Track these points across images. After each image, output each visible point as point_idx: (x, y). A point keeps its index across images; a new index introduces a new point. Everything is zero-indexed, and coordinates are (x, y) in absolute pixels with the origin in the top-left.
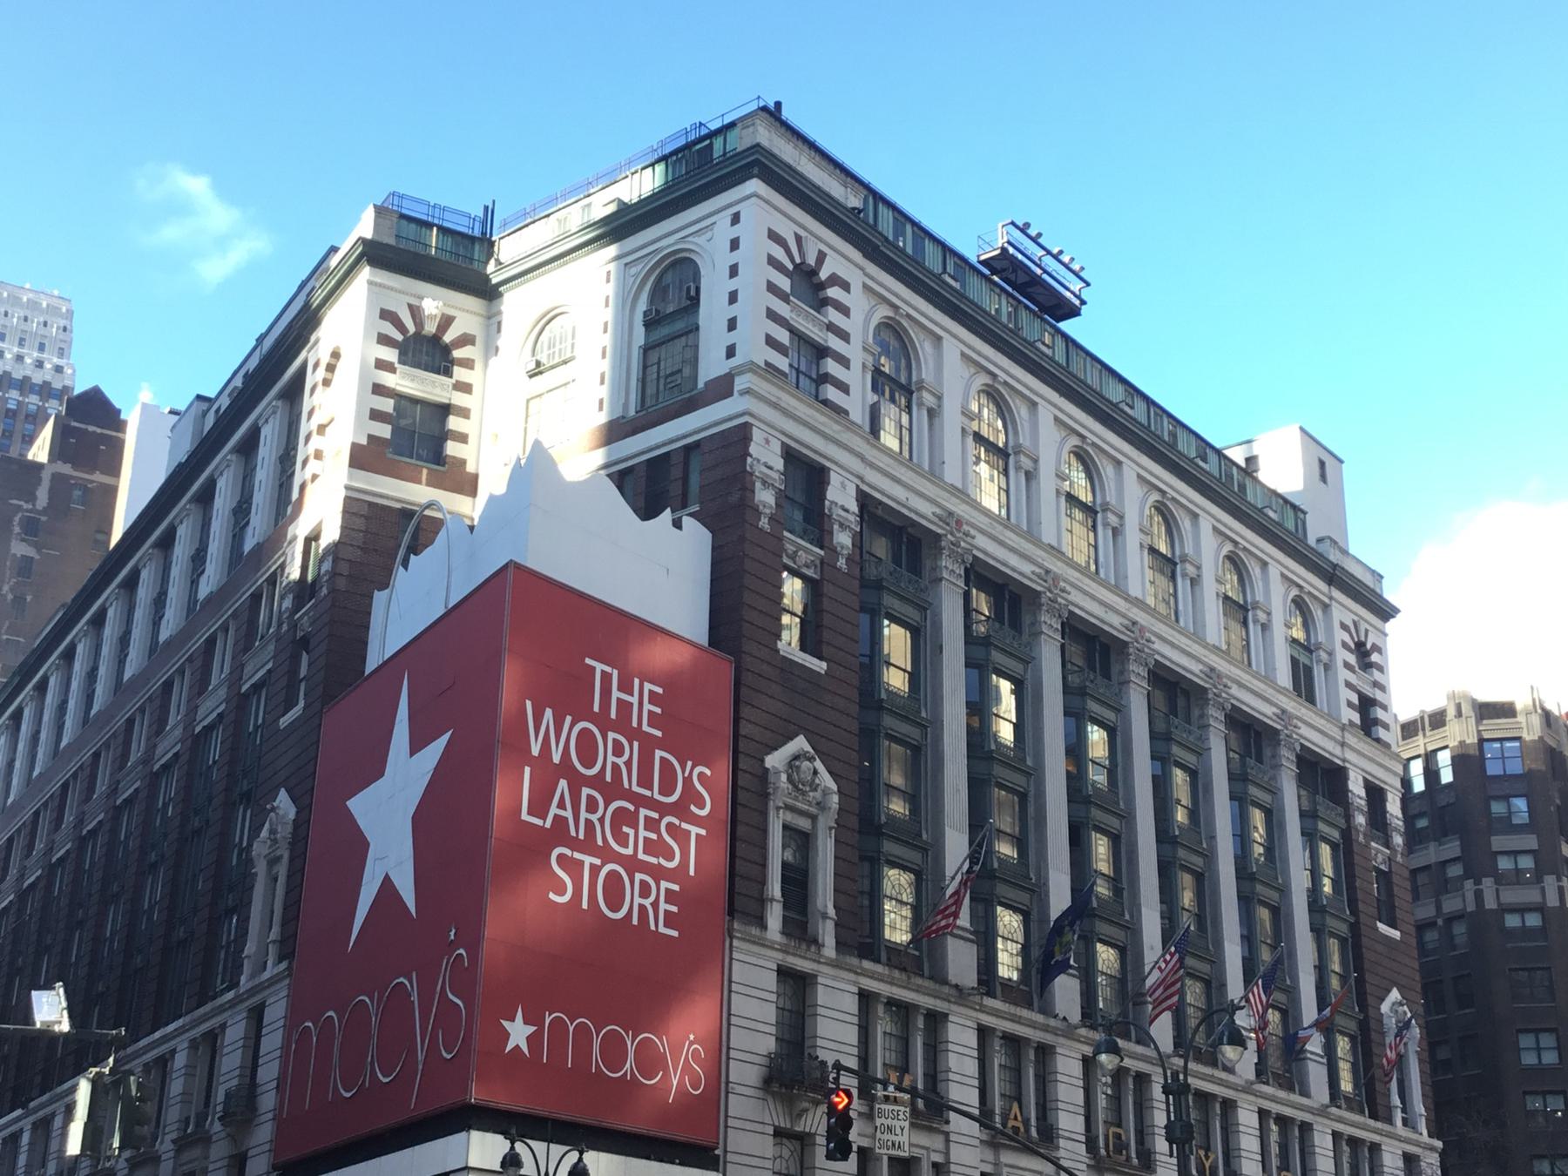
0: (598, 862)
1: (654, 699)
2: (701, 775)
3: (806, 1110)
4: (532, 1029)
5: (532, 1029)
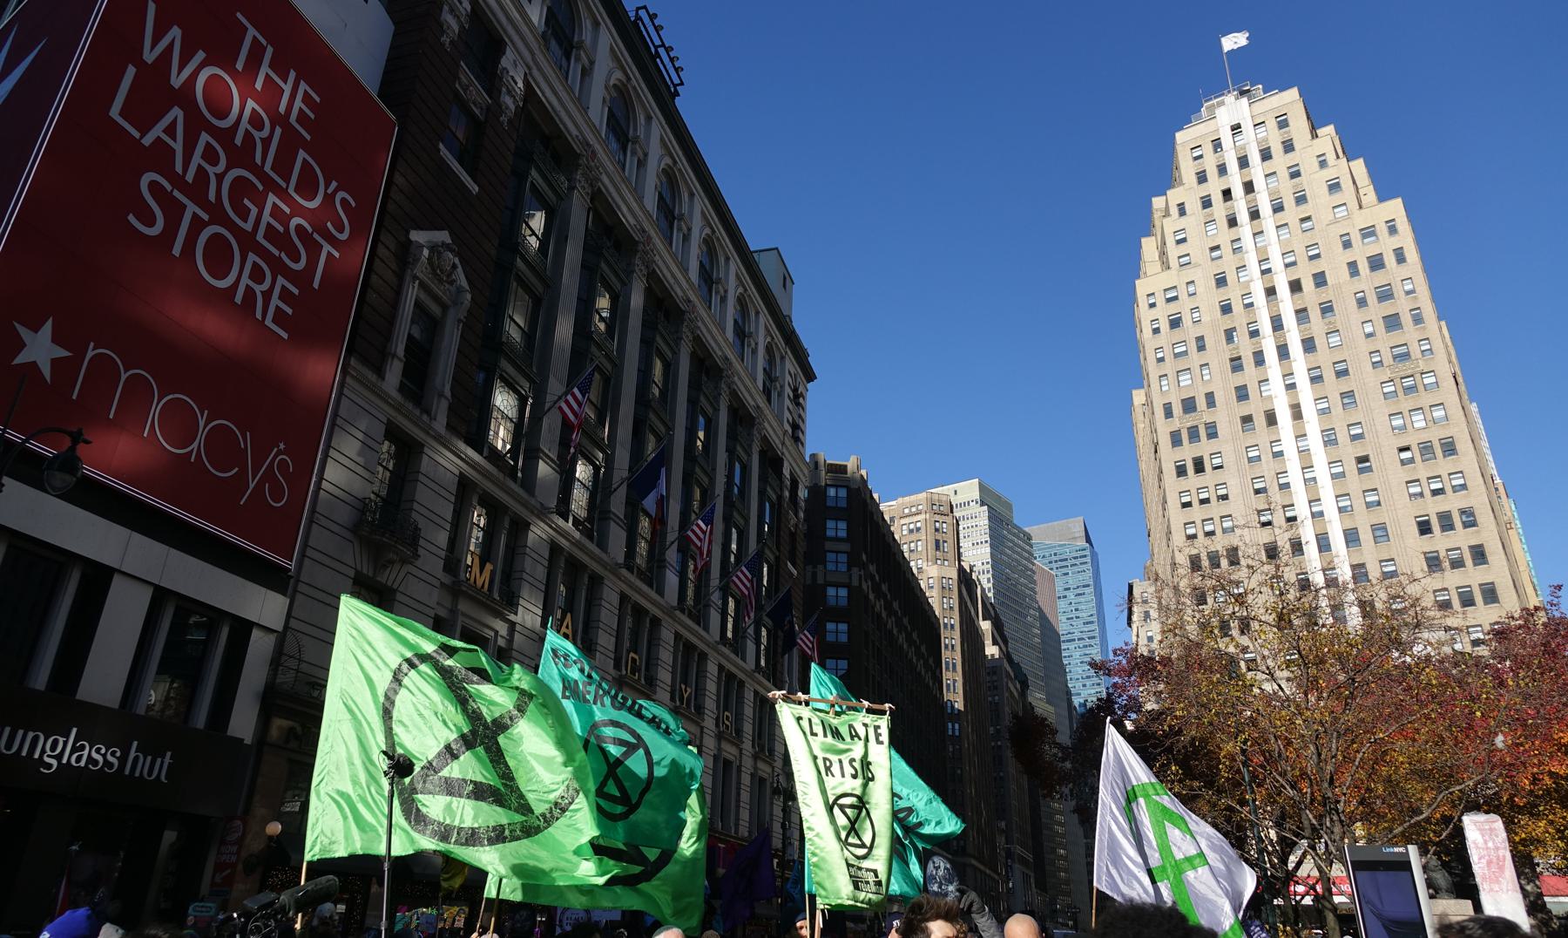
0: (206, 217)
1: (307, 98)
2: (343, 201)
3: (392, 562)
4: (65, 353)
5: (65, 353)
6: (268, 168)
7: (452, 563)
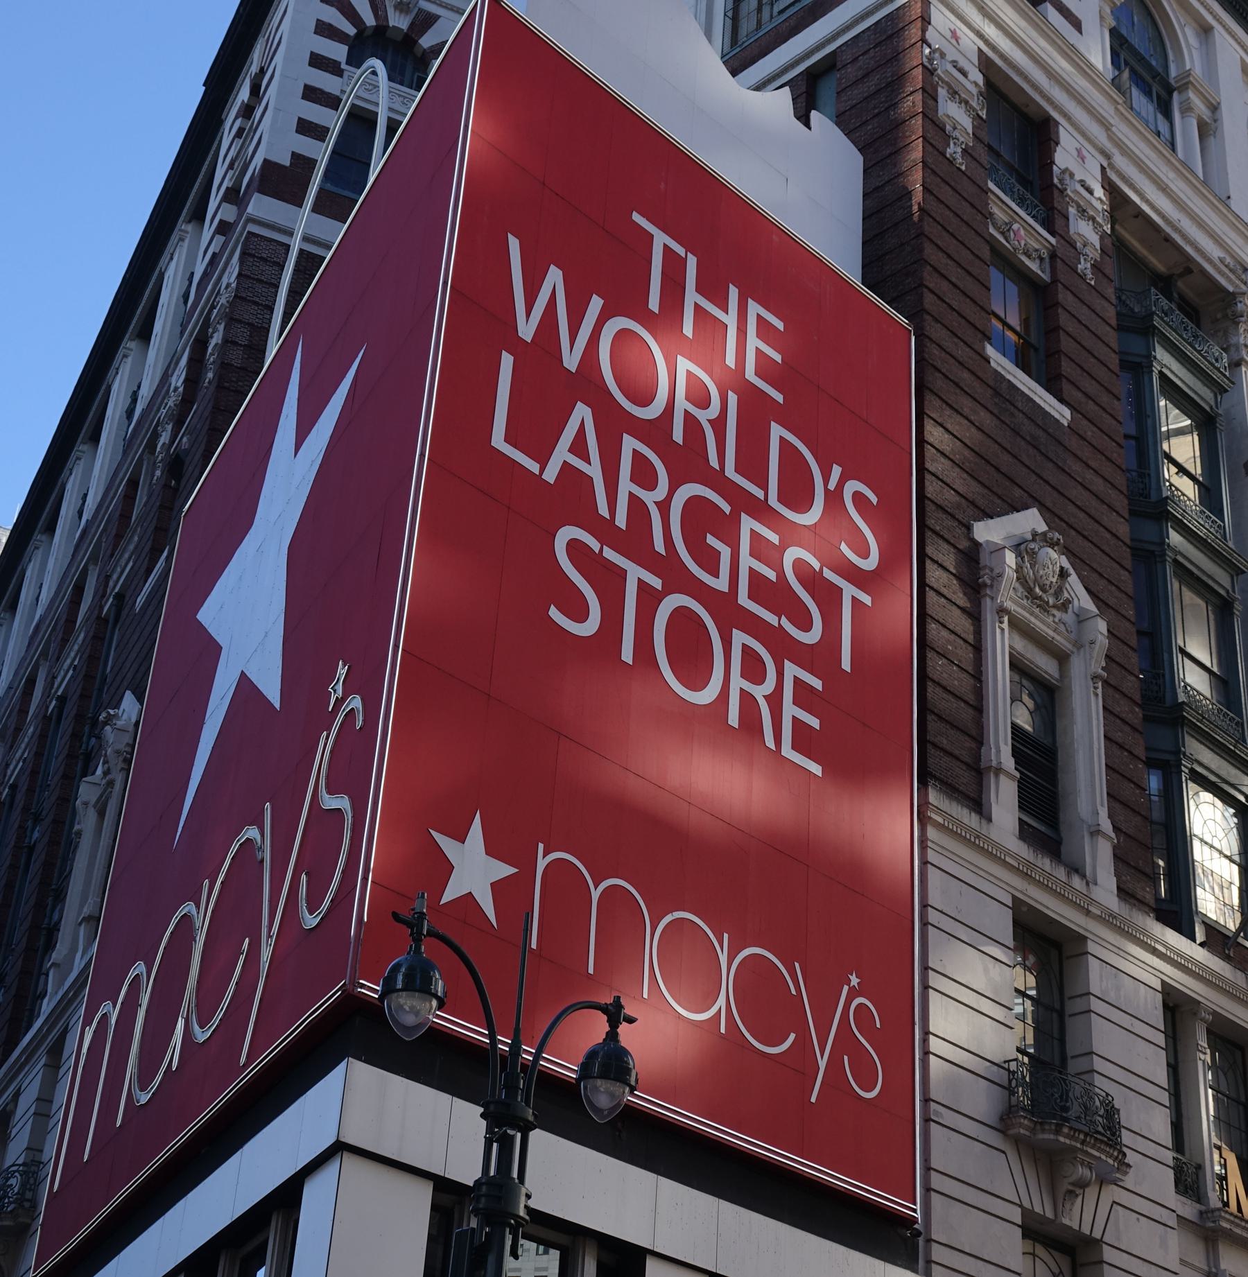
0: (656, 583)
3: (1083, 1185)
6: (730, 472)
7: (1189, 1180)
